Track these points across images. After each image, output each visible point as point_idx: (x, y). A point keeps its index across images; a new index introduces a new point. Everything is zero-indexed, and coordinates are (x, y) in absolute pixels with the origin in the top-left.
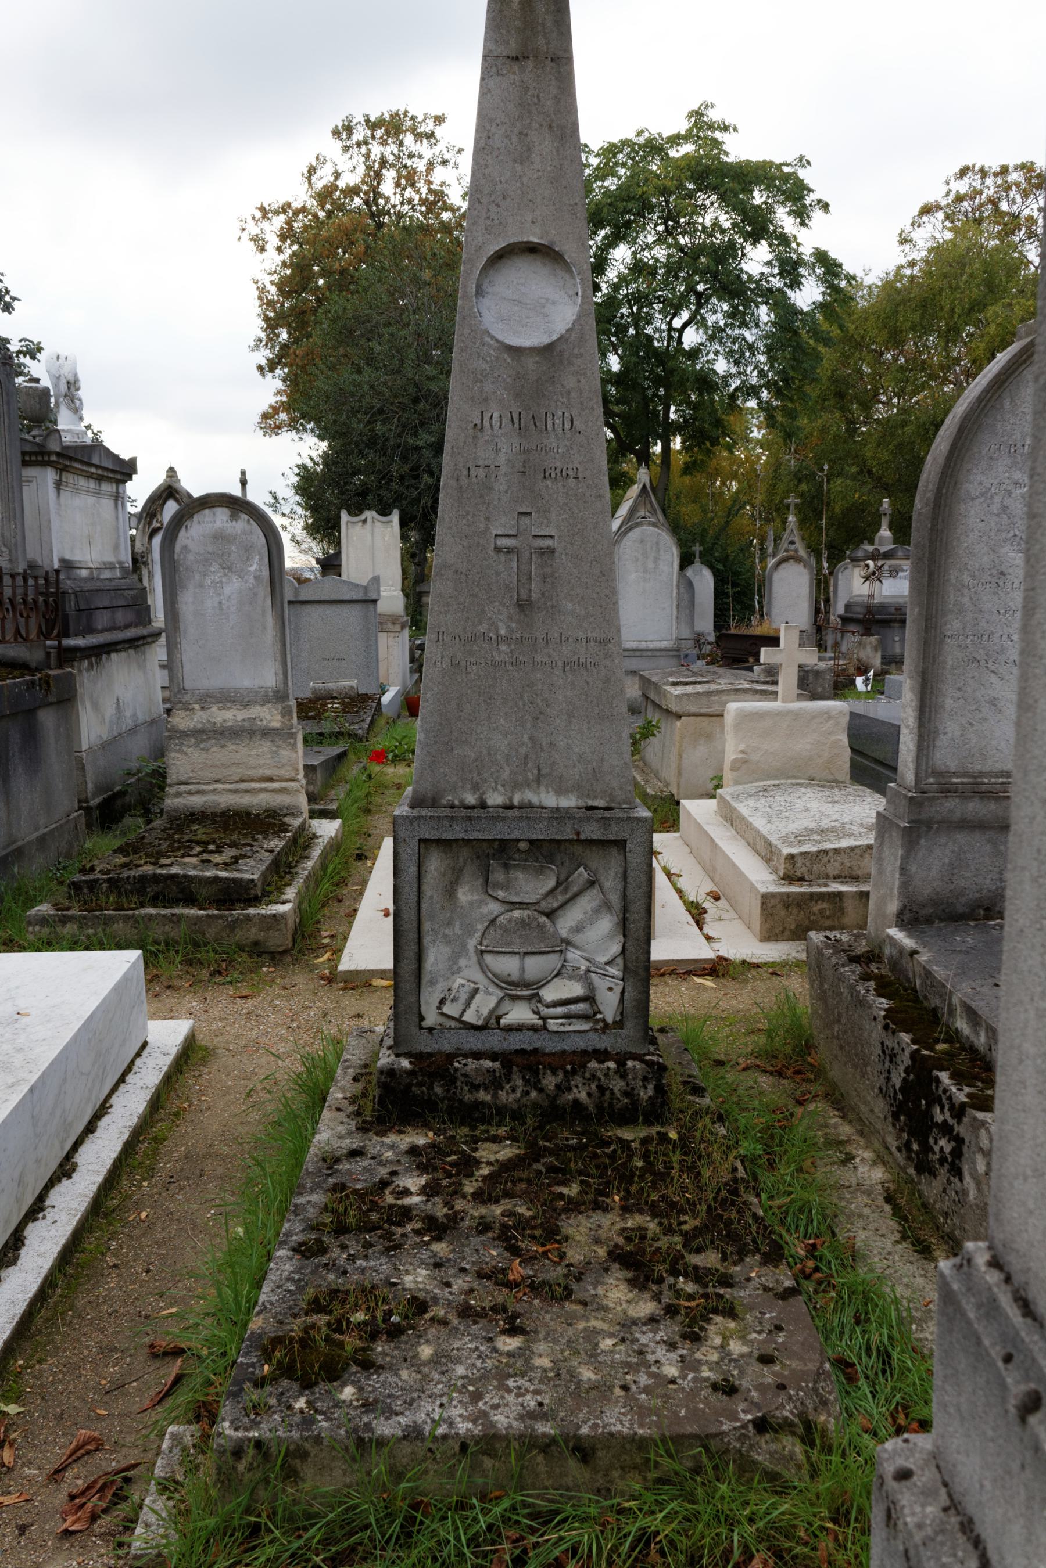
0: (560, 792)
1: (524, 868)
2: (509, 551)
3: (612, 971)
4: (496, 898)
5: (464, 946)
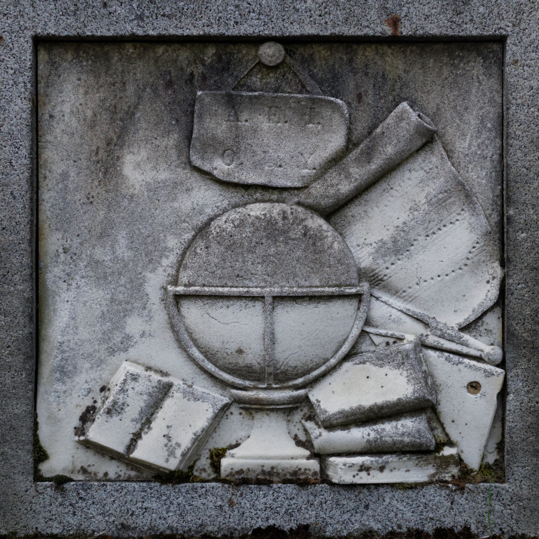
1: (274, 107)
4: (207, 175)
5: (137, 286)
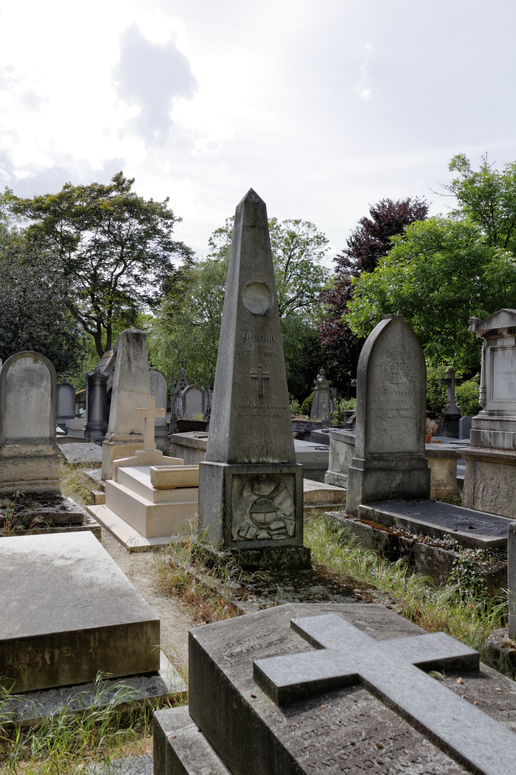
0: (274, 458)
2: (256, 378)
3: (292, 518)
4: (256, 494)
5: (245, 511)
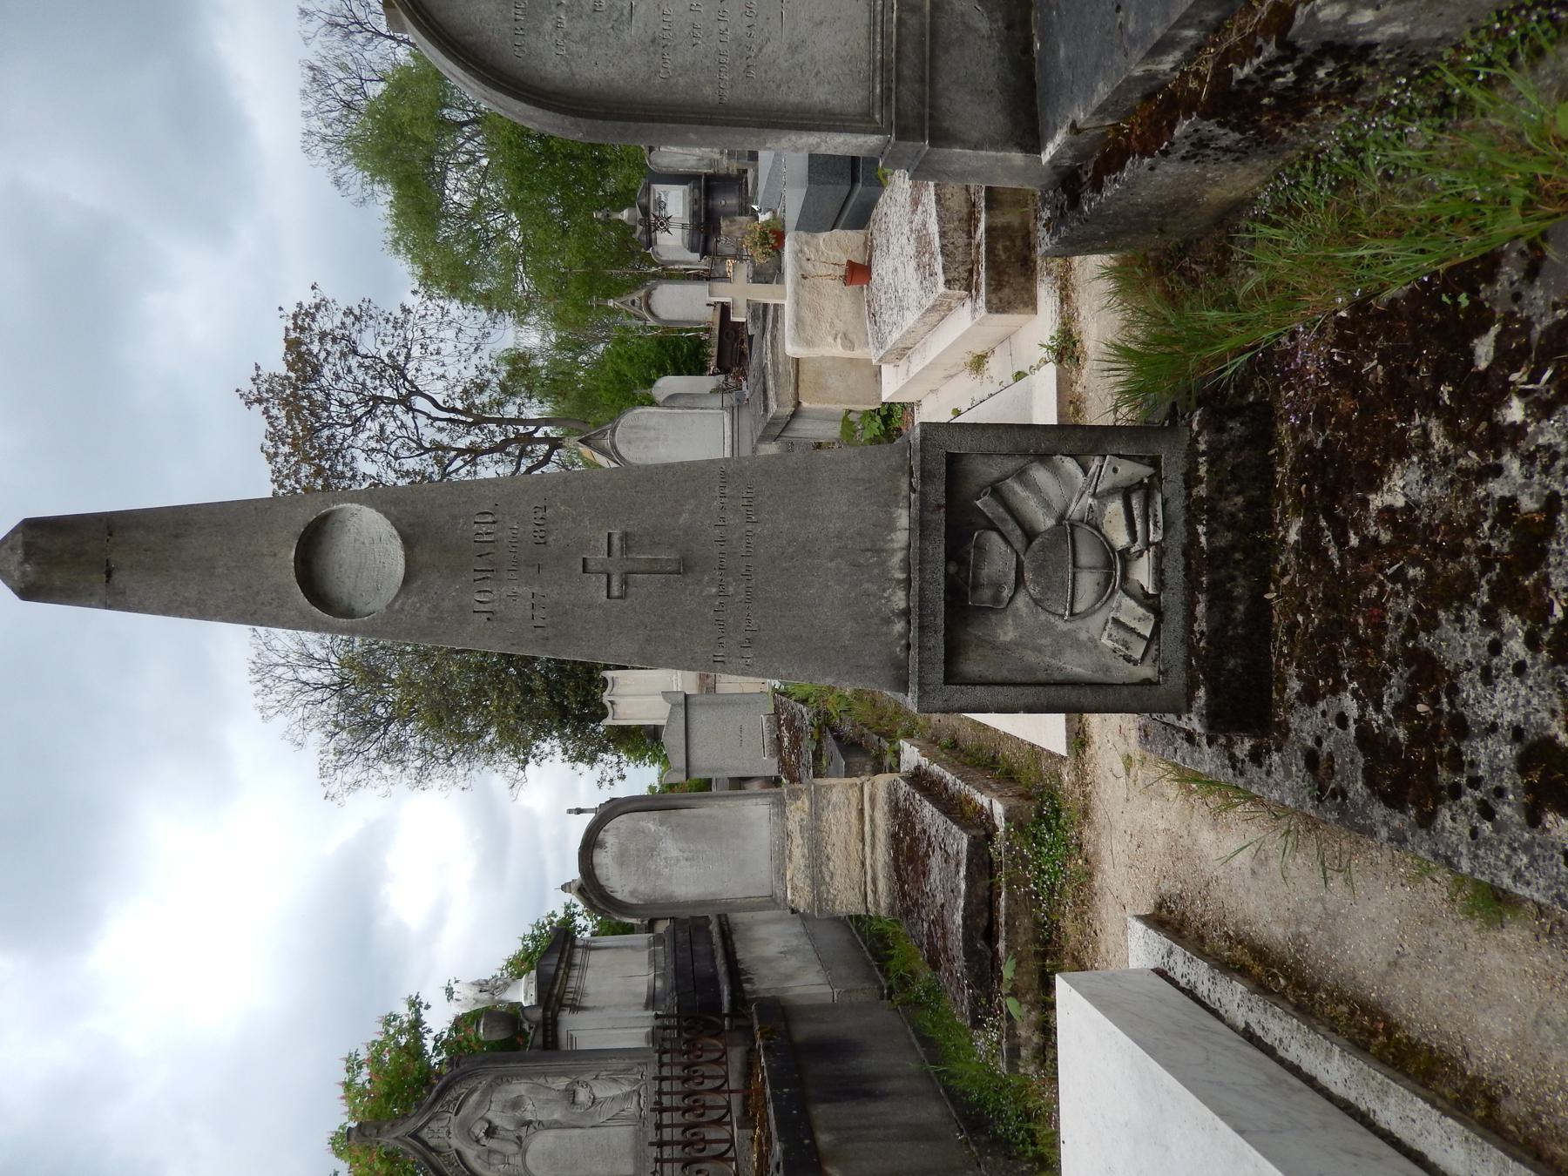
0: (891, 526)
1: (977, 567)
2: (625, 582)
4: (1011, 599)
5: (1065, 634)
